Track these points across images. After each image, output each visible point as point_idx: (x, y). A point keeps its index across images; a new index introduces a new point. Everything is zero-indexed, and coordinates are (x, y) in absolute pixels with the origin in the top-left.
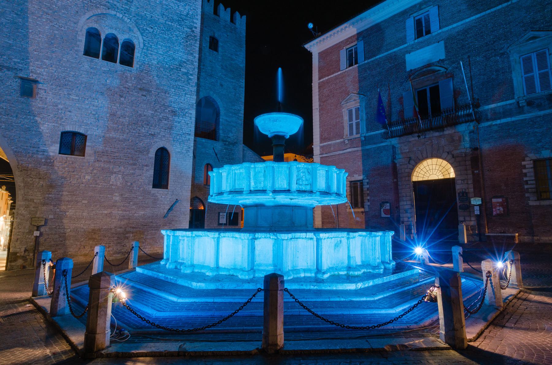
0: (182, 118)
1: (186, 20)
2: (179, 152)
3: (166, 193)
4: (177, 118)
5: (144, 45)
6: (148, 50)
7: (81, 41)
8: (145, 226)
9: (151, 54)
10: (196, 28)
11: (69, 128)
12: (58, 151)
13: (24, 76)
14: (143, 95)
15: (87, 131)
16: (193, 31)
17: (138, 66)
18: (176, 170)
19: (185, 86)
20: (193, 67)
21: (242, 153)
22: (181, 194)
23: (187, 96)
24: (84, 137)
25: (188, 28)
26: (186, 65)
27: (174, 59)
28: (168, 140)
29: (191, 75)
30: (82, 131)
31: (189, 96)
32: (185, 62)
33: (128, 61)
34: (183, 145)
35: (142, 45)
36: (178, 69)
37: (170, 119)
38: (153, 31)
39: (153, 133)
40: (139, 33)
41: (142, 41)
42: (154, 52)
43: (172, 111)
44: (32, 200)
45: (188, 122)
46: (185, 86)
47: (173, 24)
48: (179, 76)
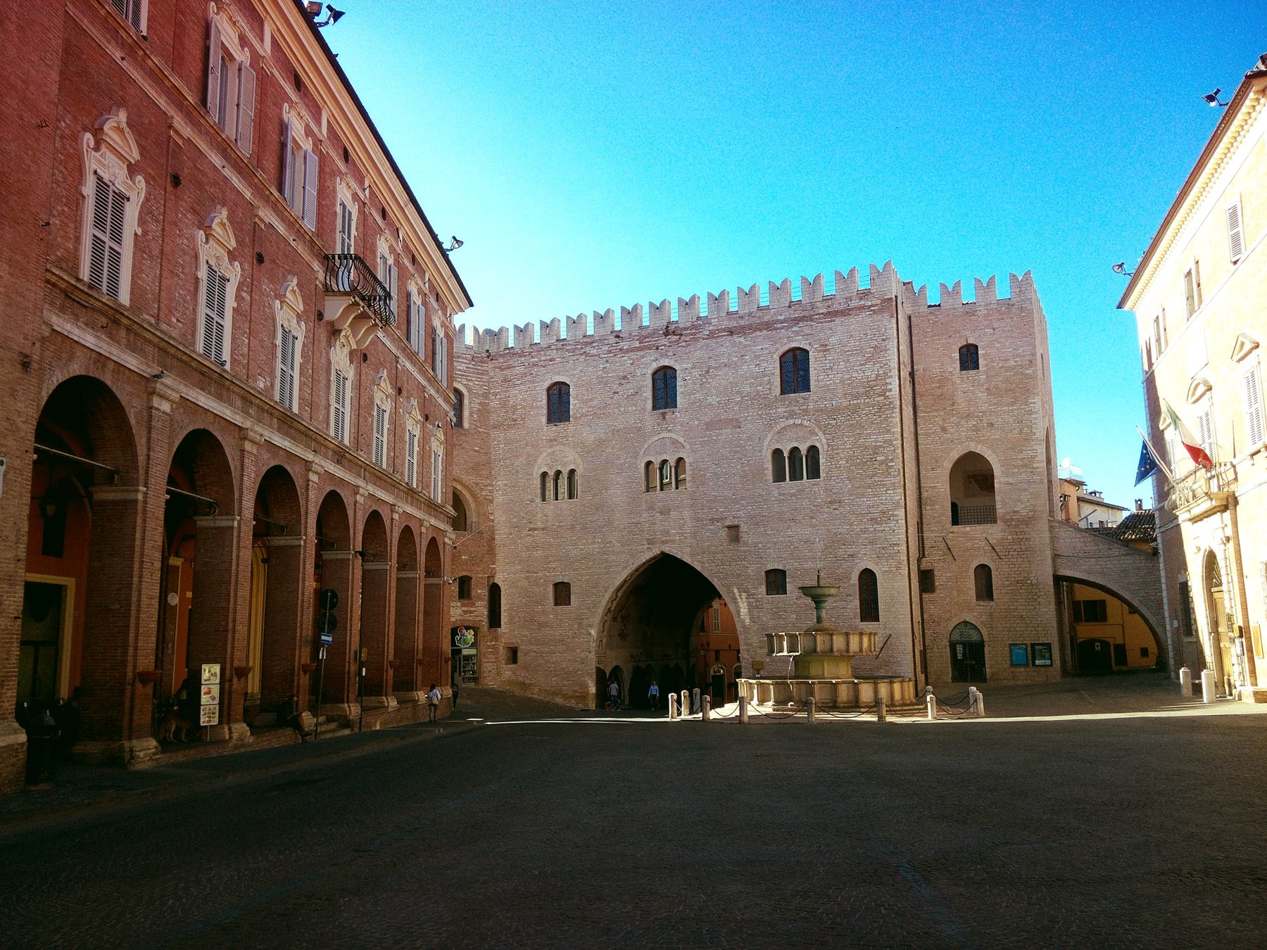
0: (885, 525)
1: (876, 386)
2: (887, 571)
3: (877, 626)
4: (879, 526)
5: (829, 446)
6: (833, 450)
7: (767, 469)
8: (858, 669)
9: (837, 454)
10: (890, 390)
11: (770, 567)
12: (765, 593)
13: (730, 523)
14: (834, 509)
15: (785, 566)
16: (887, 398)
17: (825, 475)
18: (885, 595)
19: (885, 479)
20: (893, 449)
21: (1047, 534)
22: (896, 626)
23: (888, 492)
24: (783, 573)
25: (880, 396)
26: (882, 449)
27: (866, 447)
28: (871, 558)
29: (892, 461)
30: (781, 568)
31: (892, 492)
32: (881, 446)
33: (814, 473)
34: (891, 561)
35: (826, 447)
36: (874, 459)
37: (870, 530)
38: (836, 423)
39: (851, 553)
40: (820, 433)
41: (826, 441)
42: (841, 449)
43: (872, 519)
44: (750, 645)
45: (895, 528)
46: (885, 479)
47: (859, 401)
48: (875, 468)
